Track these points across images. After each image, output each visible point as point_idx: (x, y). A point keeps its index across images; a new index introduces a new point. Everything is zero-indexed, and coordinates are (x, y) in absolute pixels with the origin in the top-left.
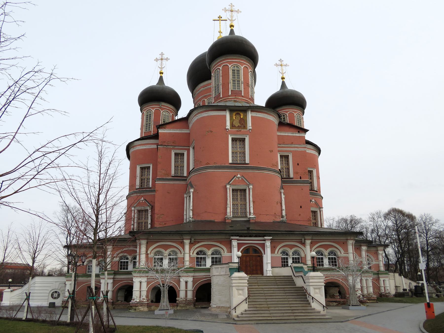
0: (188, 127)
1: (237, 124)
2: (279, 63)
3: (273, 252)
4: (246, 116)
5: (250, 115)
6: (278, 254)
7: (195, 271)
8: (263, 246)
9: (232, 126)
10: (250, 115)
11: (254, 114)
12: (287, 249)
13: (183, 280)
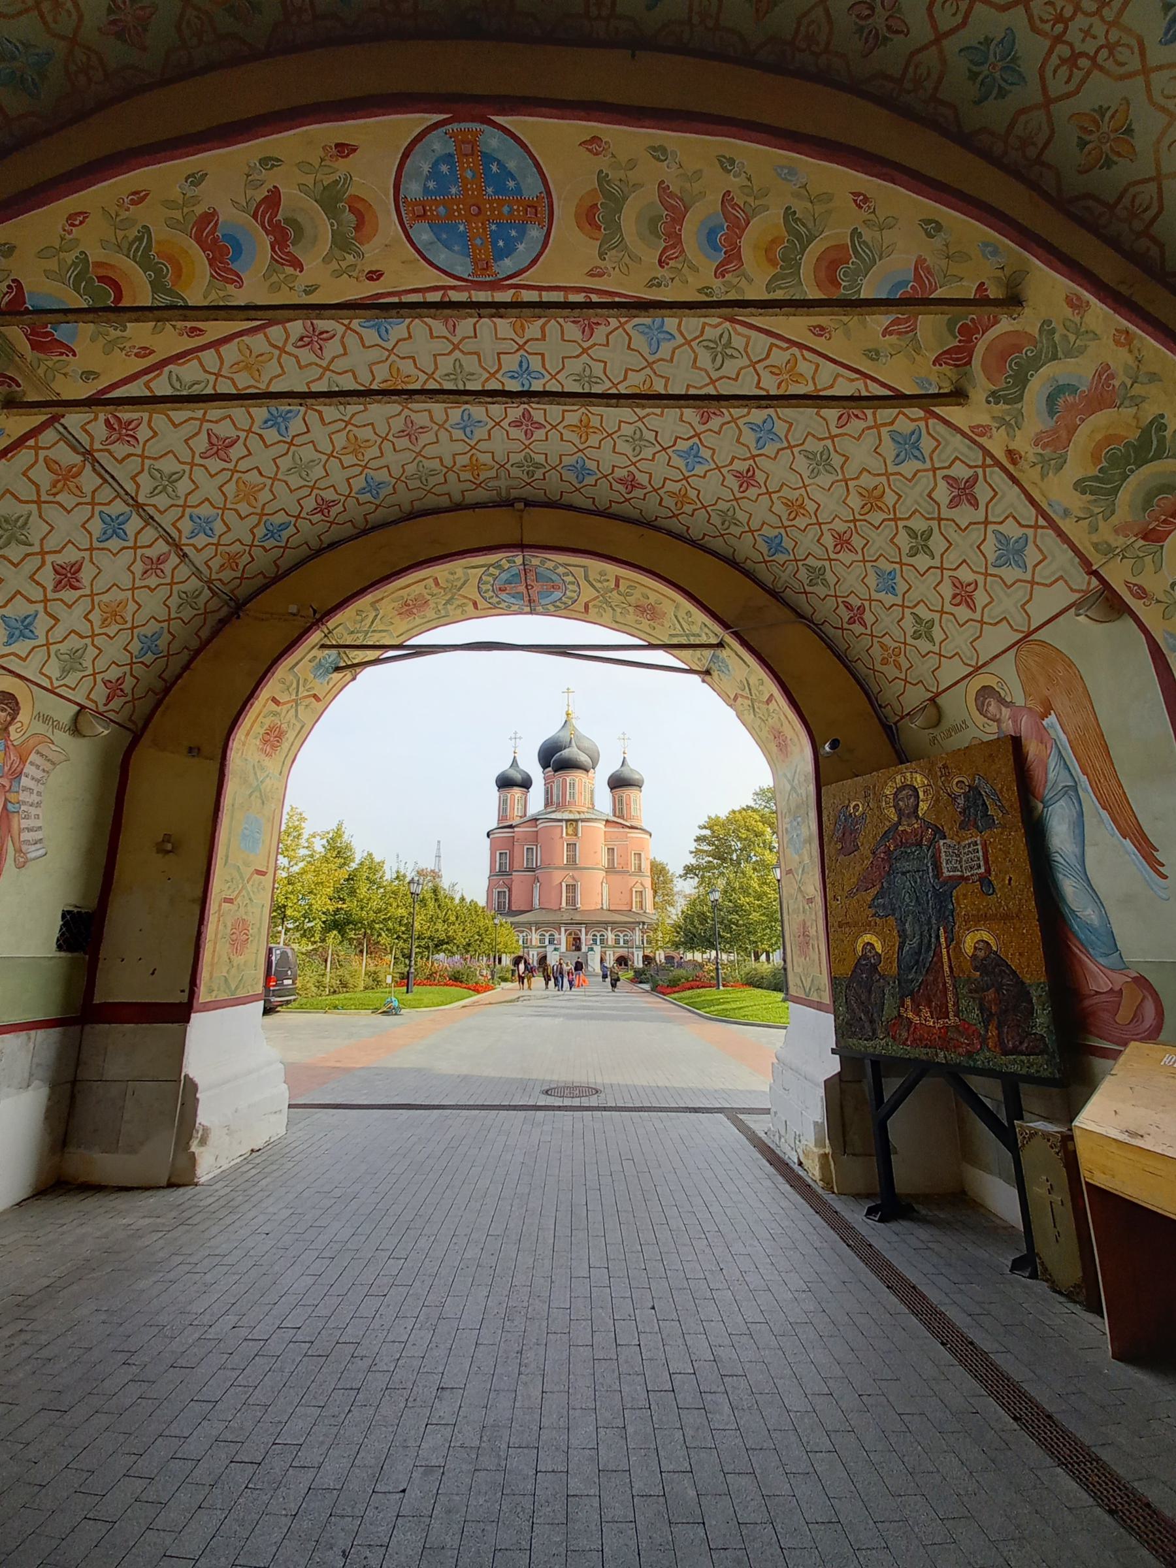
0: (536, 826)
1: (570, 832)
2: (622, 736)
3: (586, 935)
4: (577, 825)
5: (580, 824)
6: (590, 937)
7: (539, 947)
8: (580, 931)
9: (567, 834)
10: (580, 824)
11: (584, 824)
12: (596, 933)
13: (531, 953)
